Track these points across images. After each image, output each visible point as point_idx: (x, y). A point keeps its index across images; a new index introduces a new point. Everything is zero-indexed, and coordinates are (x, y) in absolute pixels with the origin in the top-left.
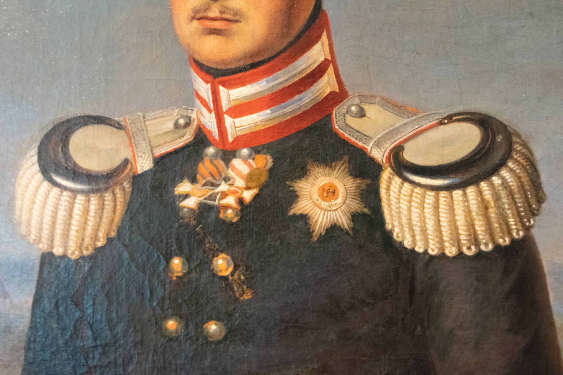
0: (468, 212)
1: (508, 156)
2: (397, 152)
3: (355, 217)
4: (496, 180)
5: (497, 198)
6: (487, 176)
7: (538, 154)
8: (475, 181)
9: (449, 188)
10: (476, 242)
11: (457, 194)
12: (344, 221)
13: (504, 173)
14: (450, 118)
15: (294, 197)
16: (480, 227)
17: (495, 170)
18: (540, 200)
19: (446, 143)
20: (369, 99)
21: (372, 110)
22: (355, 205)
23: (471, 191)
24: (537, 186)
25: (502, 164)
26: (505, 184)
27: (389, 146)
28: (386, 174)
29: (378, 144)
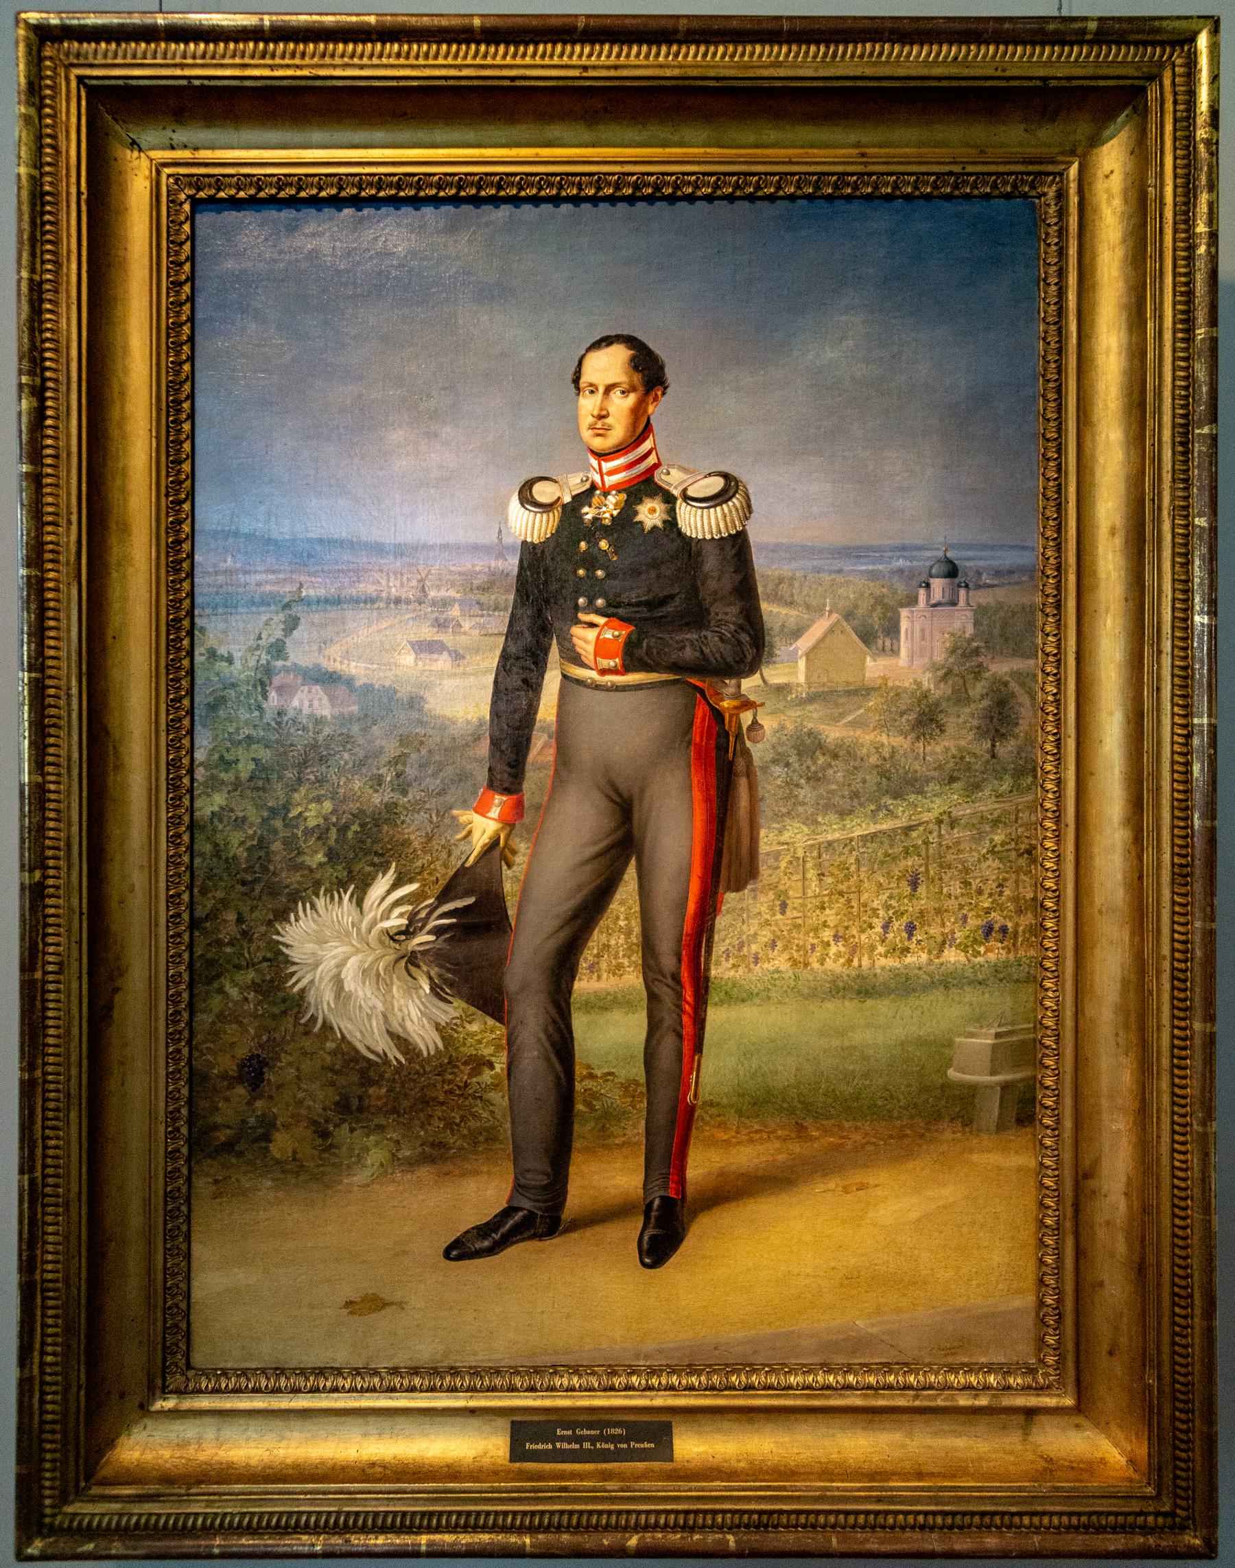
0: (717, 518)
1: (736, 492)
2: (685, 490)
3: (665, 522)
4: (730, 503)
5: (730, 512)
6: (726, 502)
7: (750, 491)
8: (720, 504)
9: (708, 508)
10: (720, 532)
11: (712, 510)
12: (660, 524)
13: (734, 500)
14: (710, 475)
15: (636, 513)
16: (722, 526)
17: (730, 499)
18: (750, 512)
19: (707, 486)
20: (672, 466)
21: (673, 472)
22: (665, 517)
23: (718, 509)
24: (749, 506)
25: (734, 496)
26: (734, 505)
27: (681, 488)
28: (679, 502)
29: (676, 488)
